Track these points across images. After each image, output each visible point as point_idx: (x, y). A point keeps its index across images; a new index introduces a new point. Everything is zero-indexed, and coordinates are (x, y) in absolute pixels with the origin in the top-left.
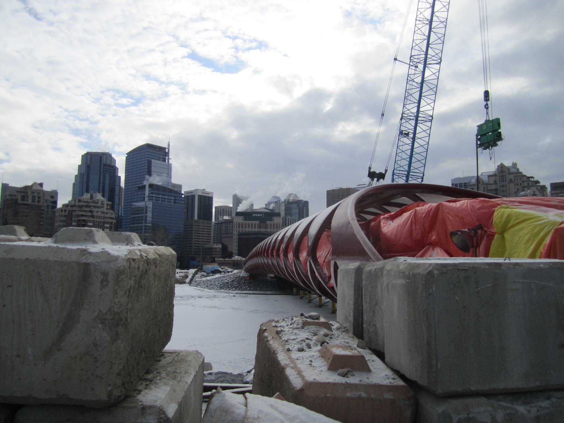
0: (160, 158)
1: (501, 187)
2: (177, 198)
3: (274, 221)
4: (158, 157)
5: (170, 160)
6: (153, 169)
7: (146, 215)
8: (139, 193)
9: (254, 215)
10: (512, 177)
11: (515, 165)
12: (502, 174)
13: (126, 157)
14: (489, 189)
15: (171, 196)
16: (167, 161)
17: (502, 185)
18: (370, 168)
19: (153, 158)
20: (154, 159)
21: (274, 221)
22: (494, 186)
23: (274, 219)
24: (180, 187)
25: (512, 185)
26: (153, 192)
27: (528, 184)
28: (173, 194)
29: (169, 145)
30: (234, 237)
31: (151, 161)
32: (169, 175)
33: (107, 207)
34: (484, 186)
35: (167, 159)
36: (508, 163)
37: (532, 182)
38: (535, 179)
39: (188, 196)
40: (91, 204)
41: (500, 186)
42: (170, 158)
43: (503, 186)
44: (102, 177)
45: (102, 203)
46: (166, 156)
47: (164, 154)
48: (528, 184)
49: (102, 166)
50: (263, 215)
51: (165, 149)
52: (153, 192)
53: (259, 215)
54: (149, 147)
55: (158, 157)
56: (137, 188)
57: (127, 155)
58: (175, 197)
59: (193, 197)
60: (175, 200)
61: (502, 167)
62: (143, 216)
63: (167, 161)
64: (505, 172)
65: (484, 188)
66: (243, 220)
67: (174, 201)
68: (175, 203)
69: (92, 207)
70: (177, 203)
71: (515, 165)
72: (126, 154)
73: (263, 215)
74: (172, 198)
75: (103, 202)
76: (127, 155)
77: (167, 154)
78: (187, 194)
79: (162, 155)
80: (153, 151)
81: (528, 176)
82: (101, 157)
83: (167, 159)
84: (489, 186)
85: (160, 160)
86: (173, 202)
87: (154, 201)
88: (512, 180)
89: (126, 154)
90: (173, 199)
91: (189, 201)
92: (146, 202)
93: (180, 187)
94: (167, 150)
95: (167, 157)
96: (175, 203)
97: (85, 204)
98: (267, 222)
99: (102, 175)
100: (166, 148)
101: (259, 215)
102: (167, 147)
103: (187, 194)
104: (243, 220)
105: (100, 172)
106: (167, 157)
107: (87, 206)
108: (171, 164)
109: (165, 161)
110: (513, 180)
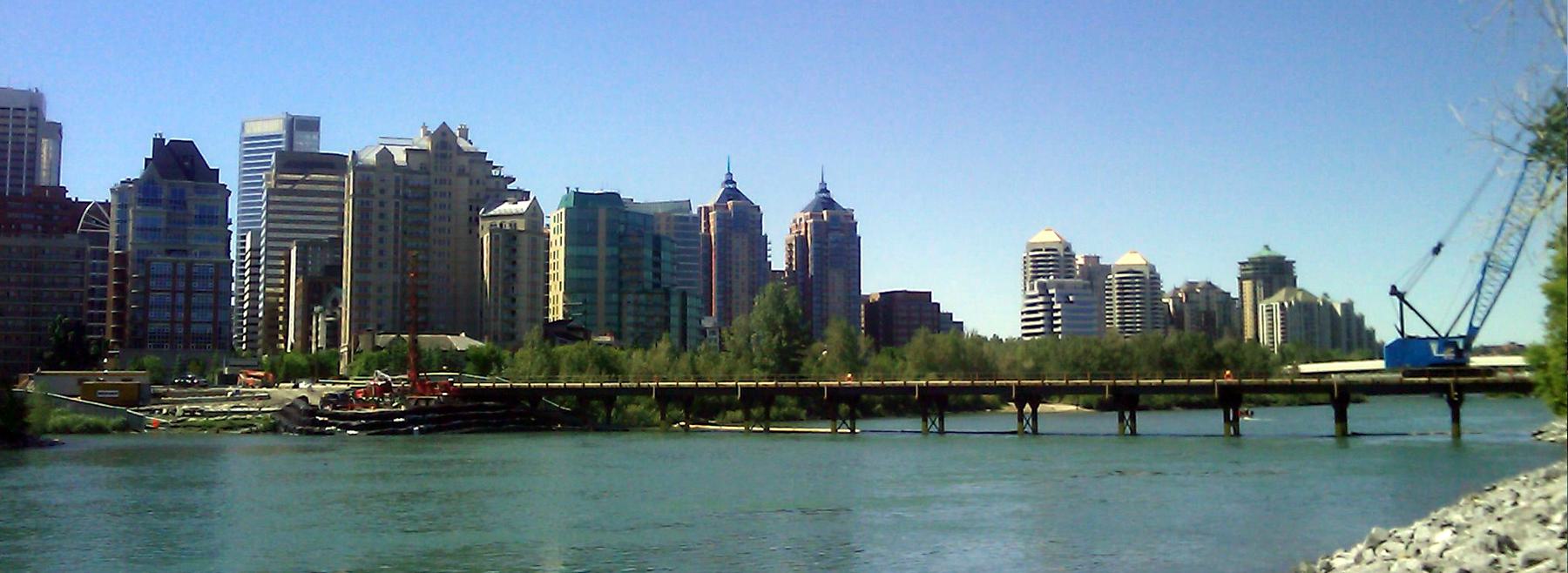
1: (438, 182)
10: (464, 161)
12: (444, 152)
14: (411, 183)
17: (441, 180)
18: (425, 127)
22: (423, 177)
25: (465, 181)
34: (398, 174)
38: (505, 173)
41: (436, 181)
43: (443, 181)
64: (451, 149)
84: (408, 176)
88: (464, 170)
110: (467, 170)
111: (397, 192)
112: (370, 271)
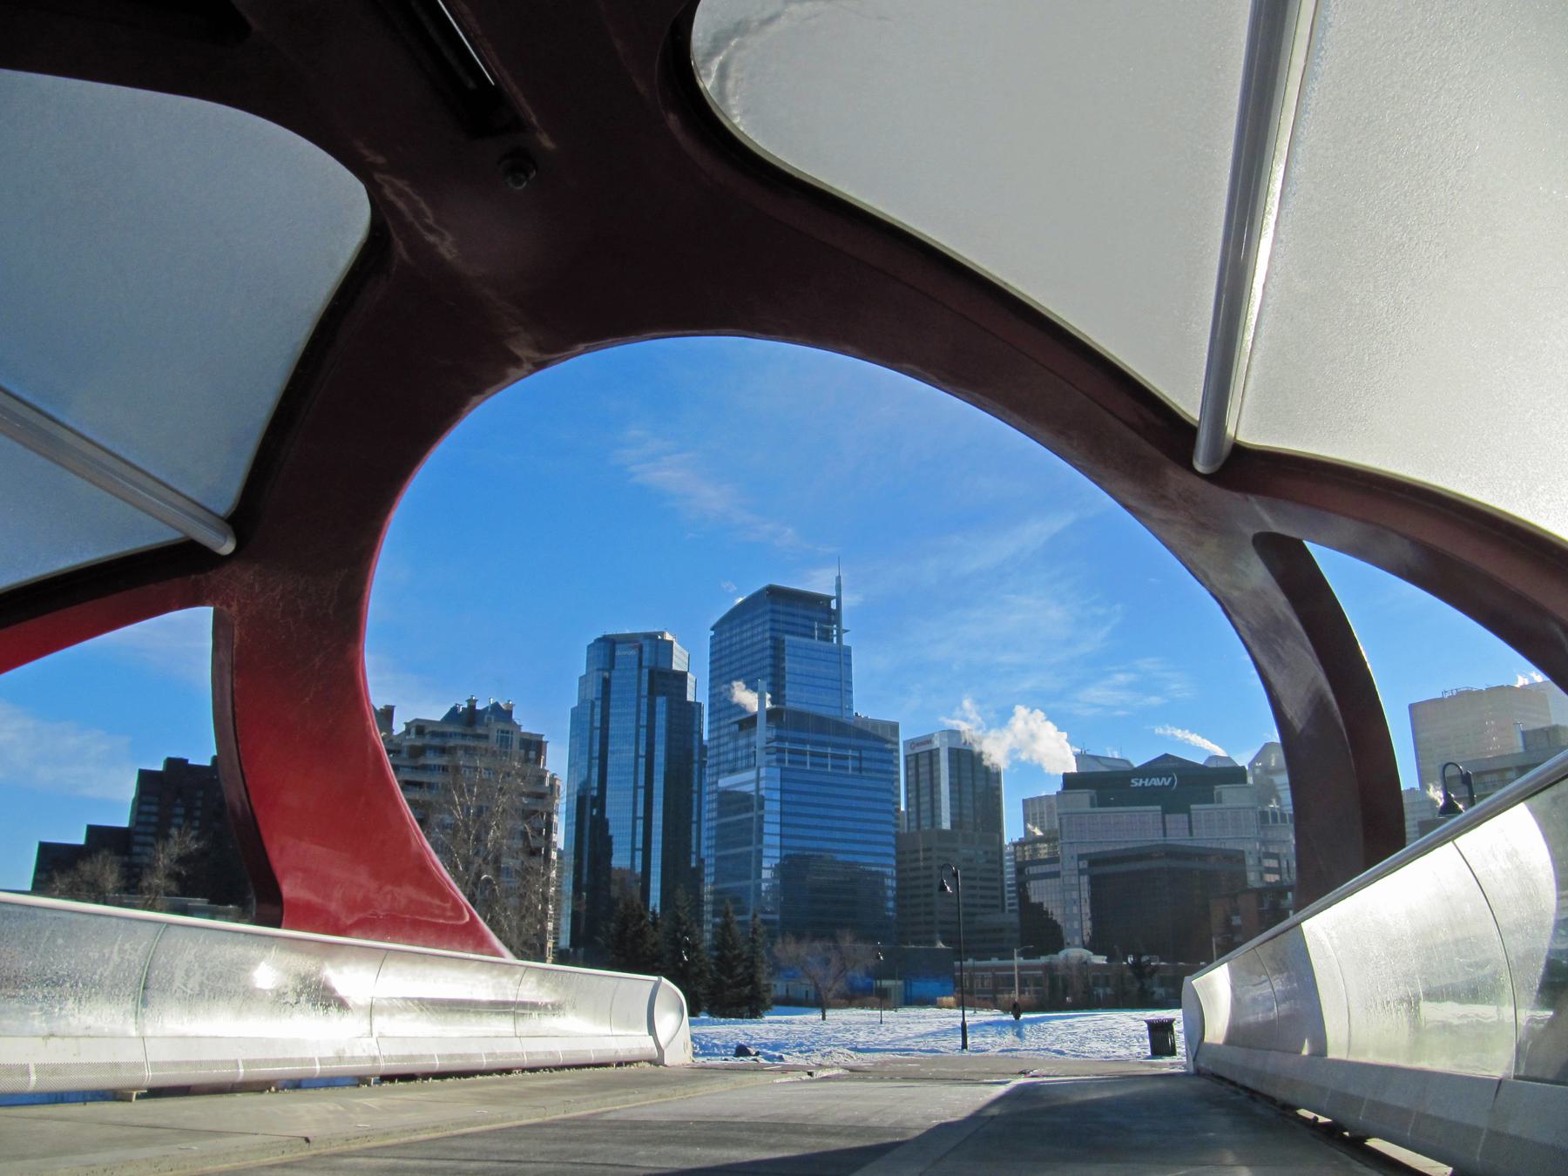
0: (813, 629)
2: (865, 754)
3: (1220, 802)
4: (805, 626)
5: (844, 636)
6: (788, 665)
7: (760, 813)
8: (742, 742)
9: (1136, 783)
13: (711, 638)
15: (845, 747)
16: (835, 639)
19: (788, 632)
20: (793, 633)
21: (1220, 802)
23: (1220, 794)
24: (894, 728)
26: (785, 733)
28: (854, 742)
29: (839, 588)
30: (1062, 873)
31: (784, 641)
32: (843, 686)
33: (527, 753)
35: (835, 632)
39: (917, 755)
40: (451, 743)
42: (844, 627)
44: (644, 707)
45: (502, 737)
46: (830, 622)
47: (825, 616)
49: (645, 671)
50: (1173, 781)
51: (829, 599)
52: (785, 733)
53: (1156, 782)
55: (805, 626)
56: (737, 726)
57: (713, 633)
58: (859, 749)
59: (933, 755)
60: (860, 759)
62: (751, 819)
63: (835, 639)
66: (1092, 805)
67: (857, 764)
68: (860, 769)
69: (460, 753)
70: (867, 770)
72: (712, 629)
73: (1173, 781)
74: (850, 753)
75: (508, 732)
76: (713, 633)
77: (833, 617)
78: (913, 749)
79: (821, 621)
80: (790, 610)
82: (641, 649)
83: (835, 632)
85: (813, 637)
86: (854, 769)
87: (787, 765)
89: (712, 629)
90: (854, 758)
91: (921, 770)
92: (759, 768)
93: (894, 728)
94: (833, 605)
95: (835, 626)
96: (860, 769)
97: (436, 742)
98: (1193, 807)
99: (644, 701)
100: (833, 598)
101: (1156, 782)
102: (835, 595)
103: (913, 749)
104: (1092, 805)
105: (639, 691)
106: (835, 626)
107: (443, 751)
108: (849, 649)
109: (826, 636)
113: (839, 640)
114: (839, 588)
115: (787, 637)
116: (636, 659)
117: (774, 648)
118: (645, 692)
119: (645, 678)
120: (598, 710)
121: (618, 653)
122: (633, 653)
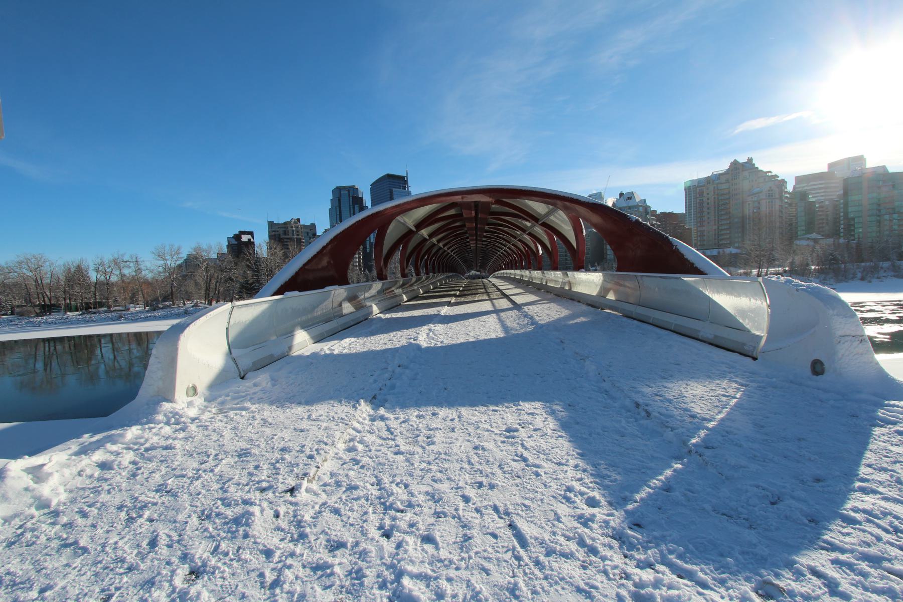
11: (750, 160)
27: (765, 179)
29: (407, 174)
36: (742, 159)
37: (769, 176)
44: (352, 208)
48: (765, 179)
49: (351, 198)
51: (404, 177)
54: (389, 176)
61: (735, 164)
65: (714, 187)
71: (750, 160)
77: (406, 182)
81: (765, 170)
82: (349, 191)
94: (406, 179)
99: (351, 206)
110: (748, 177)
111: (714, 193)
112: (704, 226)
113: (408, 189)
114: (407, 174)
115: (394, 189)
116: (348, 194)
117: (390, 192)
118: (351, 204)
119: (351, 200)
120: (338, 209)
121: (342, 192)
122: (346, 192)
